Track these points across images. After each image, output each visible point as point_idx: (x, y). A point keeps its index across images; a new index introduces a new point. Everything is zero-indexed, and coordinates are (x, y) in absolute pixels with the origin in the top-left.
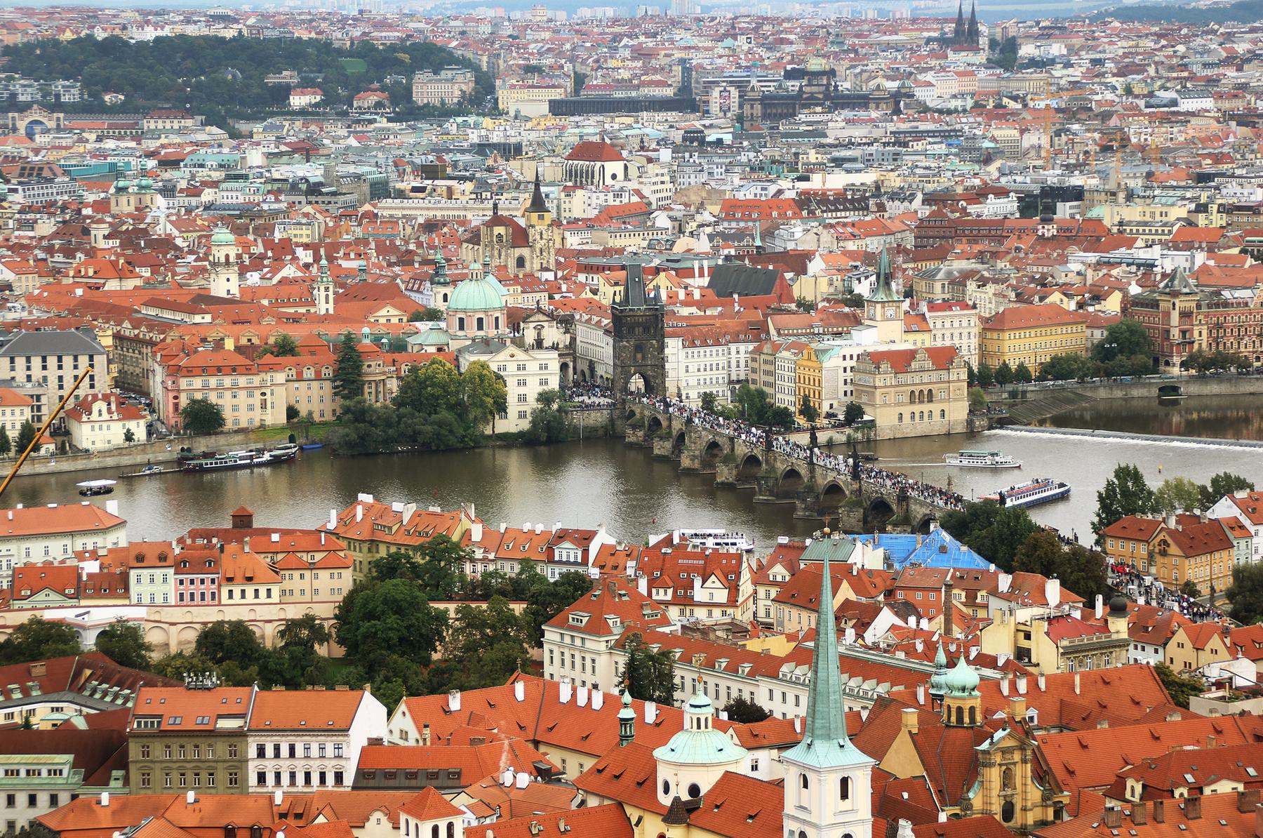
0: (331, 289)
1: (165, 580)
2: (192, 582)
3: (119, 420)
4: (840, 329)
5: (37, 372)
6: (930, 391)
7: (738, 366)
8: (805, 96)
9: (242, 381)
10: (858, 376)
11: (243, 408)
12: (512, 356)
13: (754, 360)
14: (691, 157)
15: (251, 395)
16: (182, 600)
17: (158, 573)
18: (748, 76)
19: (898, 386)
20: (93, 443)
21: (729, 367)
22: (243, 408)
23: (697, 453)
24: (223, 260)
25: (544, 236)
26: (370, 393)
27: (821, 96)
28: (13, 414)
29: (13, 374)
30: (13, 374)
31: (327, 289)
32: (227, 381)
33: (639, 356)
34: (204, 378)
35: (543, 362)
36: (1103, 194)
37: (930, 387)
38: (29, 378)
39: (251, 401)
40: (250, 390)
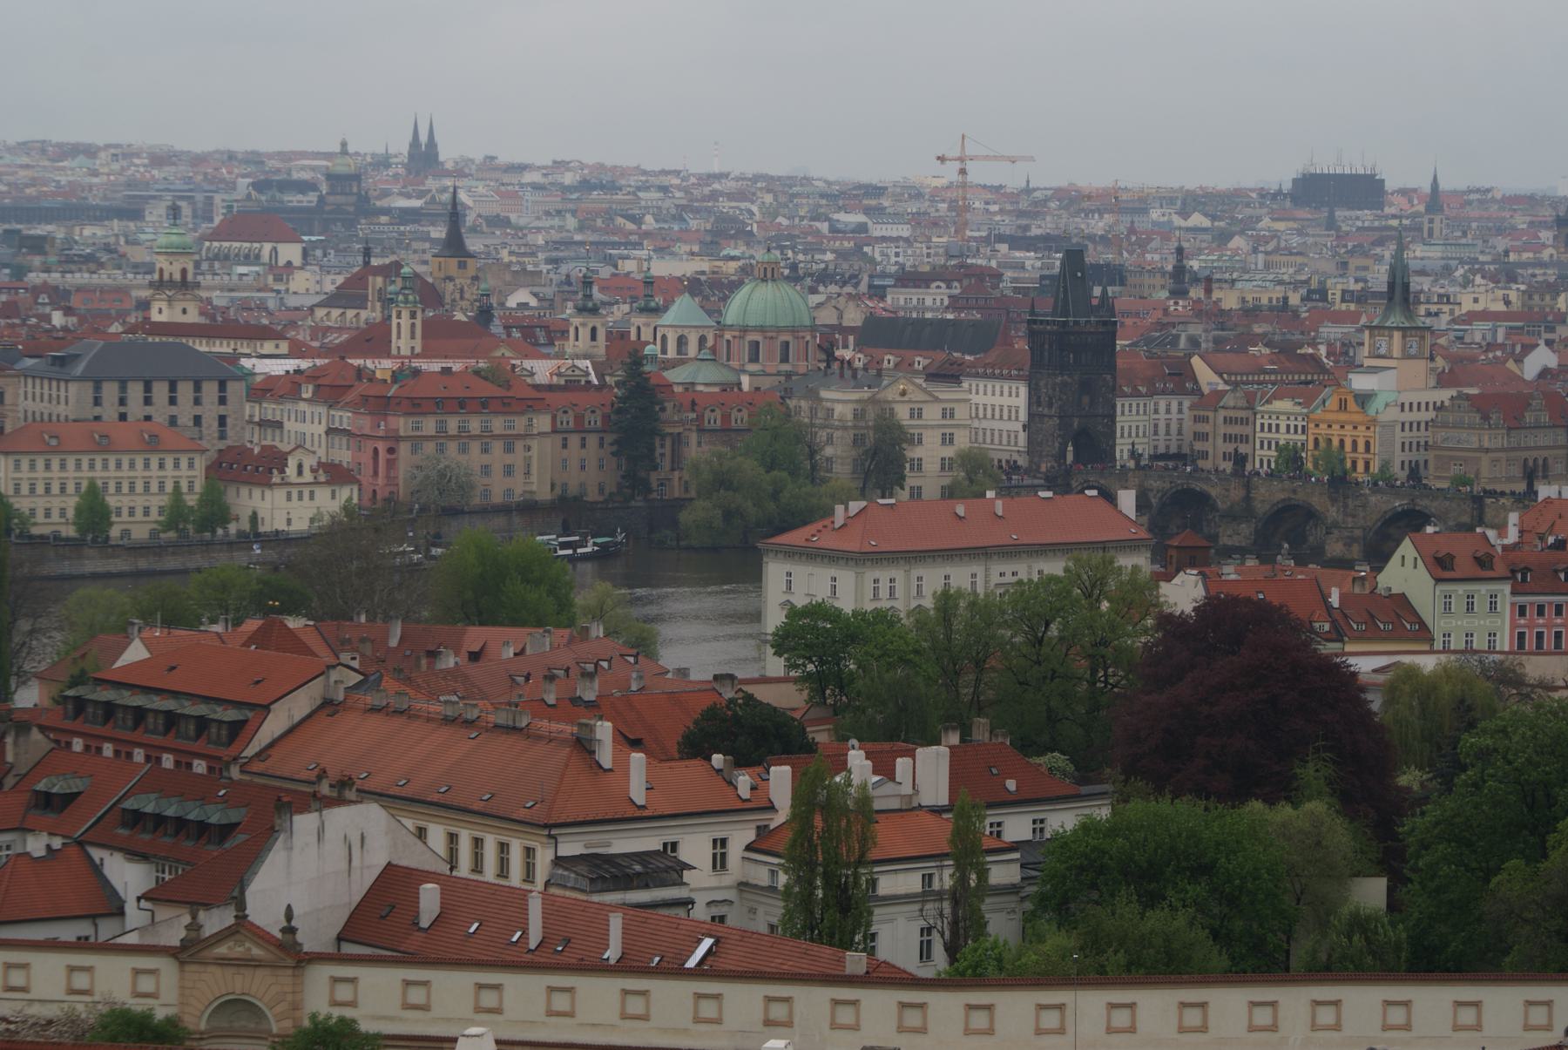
0: (419, 314)
1: (1493, 606)
2: (1541, 610)
3: (328, 483)
4: (1309, 378)
5: (135, 408)
6: (1545, 460)
7: (1168, 433)
8: (327, 208)
9: (498, 424)
10: (1442, 434)
11: (497, 469)
12: (903, 393)
13: (1197, 419)
14: (325, 255)
15: (509, 449)
16: (1521, 645)
17: (1483, 589)
18: (191, 190)
19: (1513, 449)
20: (289, 522)
21: (1156, 433)
22: (497, 469)
23: (1358, 533)
24: (177, 277)
25: (467, 296)
26: (662, 455)
27: (351, 209)
28: (161, 466)
29: (97, 411)
30: (97, 411)
31: (413, 315)
32: (475, 425)
33: (1086, 400)
34: (440, 418)
35: (948, 406)
36: (1158, 275)
37: (1545, 453)
38: (123, 417)
39: (509, 459)
40: (509, 442)
